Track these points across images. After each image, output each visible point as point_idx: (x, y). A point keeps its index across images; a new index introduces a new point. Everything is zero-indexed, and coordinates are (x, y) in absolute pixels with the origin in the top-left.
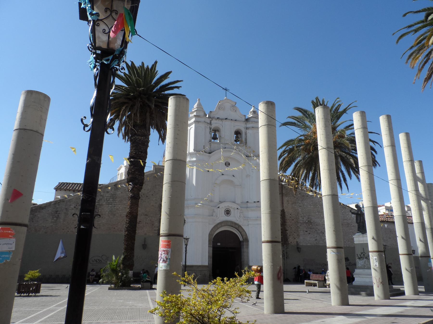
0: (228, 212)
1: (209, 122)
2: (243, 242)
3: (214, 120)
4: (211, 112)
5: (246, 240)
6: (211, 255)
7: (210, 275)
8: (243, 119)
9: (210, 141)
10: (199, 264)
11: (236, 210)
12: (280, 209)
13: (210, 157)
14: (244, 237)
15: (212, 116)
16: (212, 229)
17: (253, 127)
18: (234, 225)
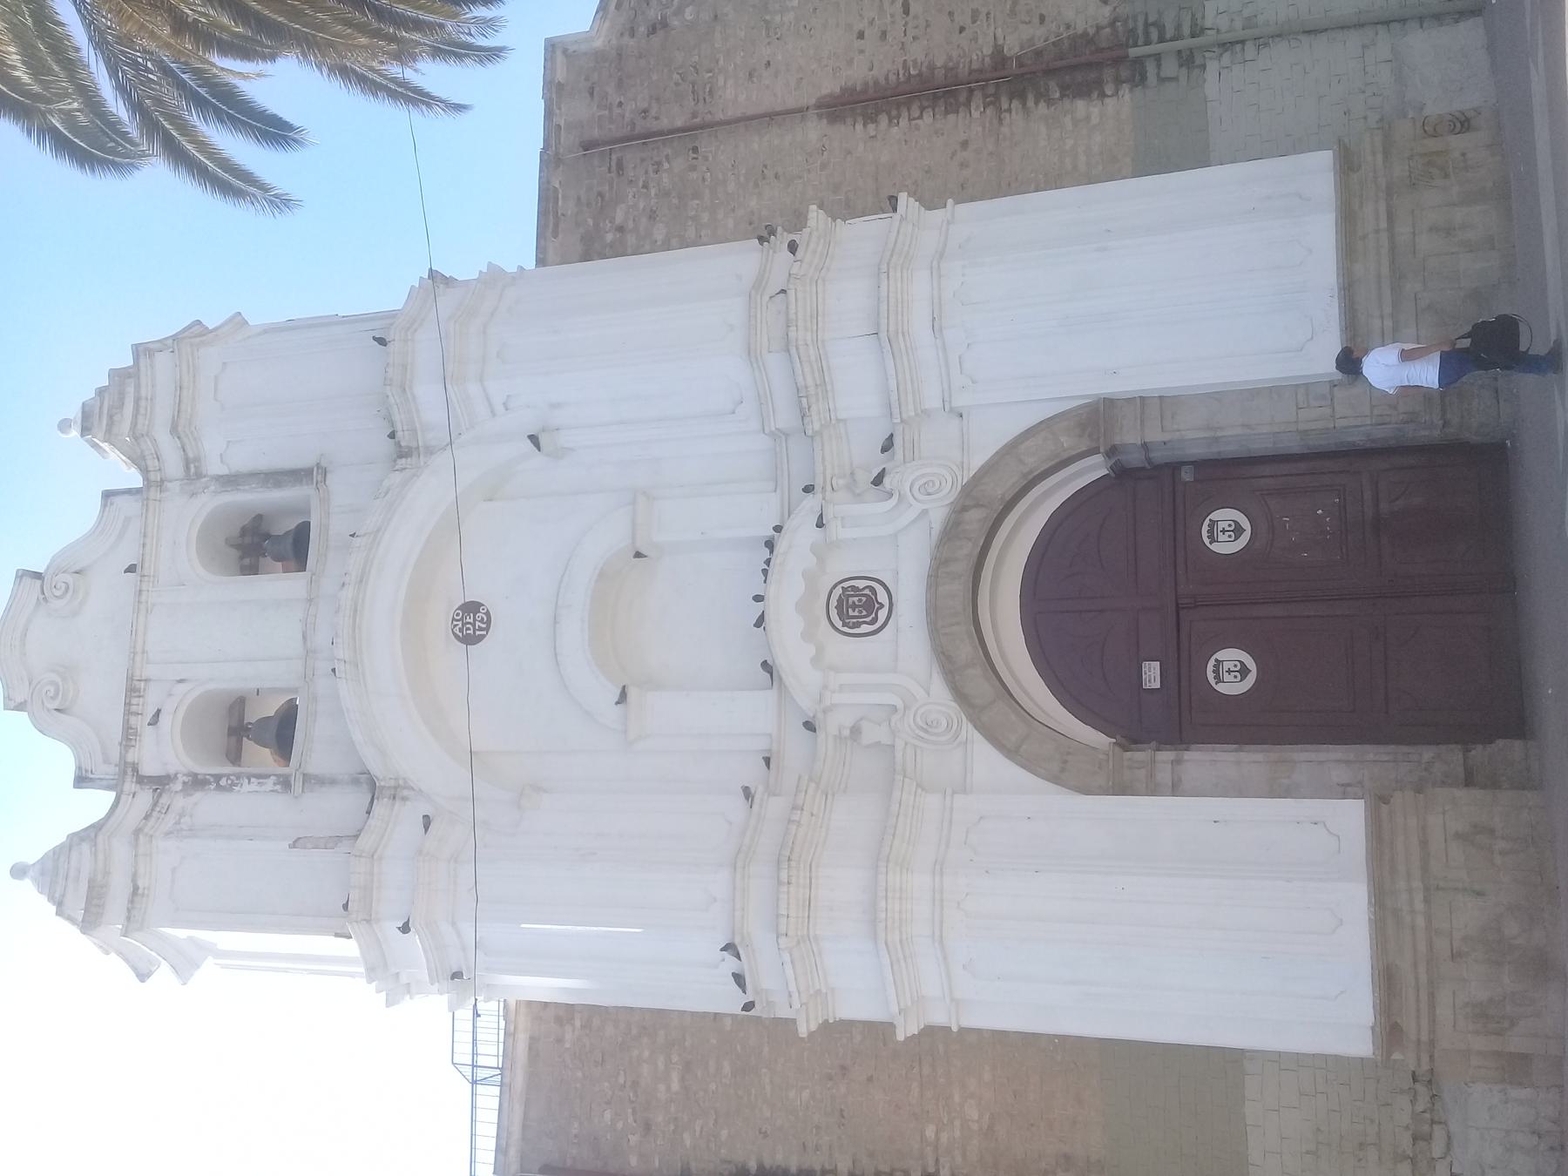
0: (858, 606)
1: (145, 797)
2: (1112, 452)
3: (131, 756)
4: (82, 780)
5: (1096, 419)
6: (1253, 760)
7: (1469, 781)
8: (129, 506)
9: (285, 783)
10: (1355, 898)
11: (835, 530)
12: (814, 131)
13: (398, 792)
14: (1068, 443)
15: (111, 770)
16: (1011, 753)
17: (174, 430)
18: (966, 550)
